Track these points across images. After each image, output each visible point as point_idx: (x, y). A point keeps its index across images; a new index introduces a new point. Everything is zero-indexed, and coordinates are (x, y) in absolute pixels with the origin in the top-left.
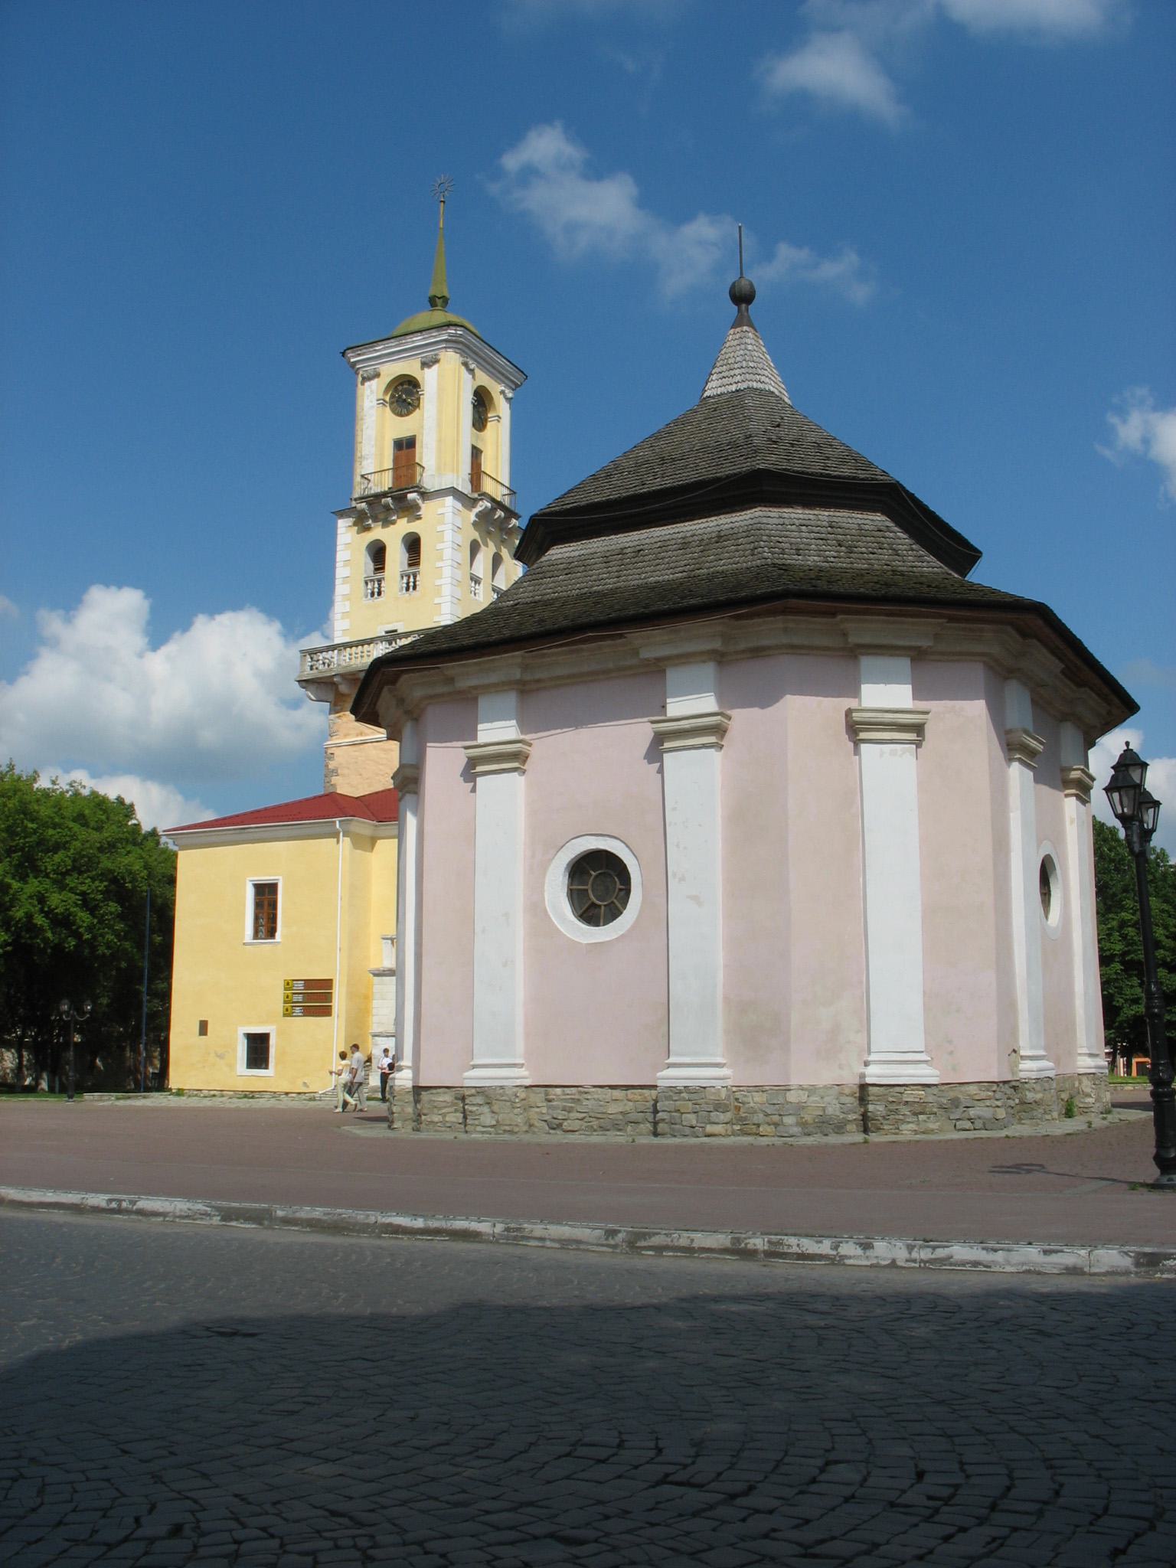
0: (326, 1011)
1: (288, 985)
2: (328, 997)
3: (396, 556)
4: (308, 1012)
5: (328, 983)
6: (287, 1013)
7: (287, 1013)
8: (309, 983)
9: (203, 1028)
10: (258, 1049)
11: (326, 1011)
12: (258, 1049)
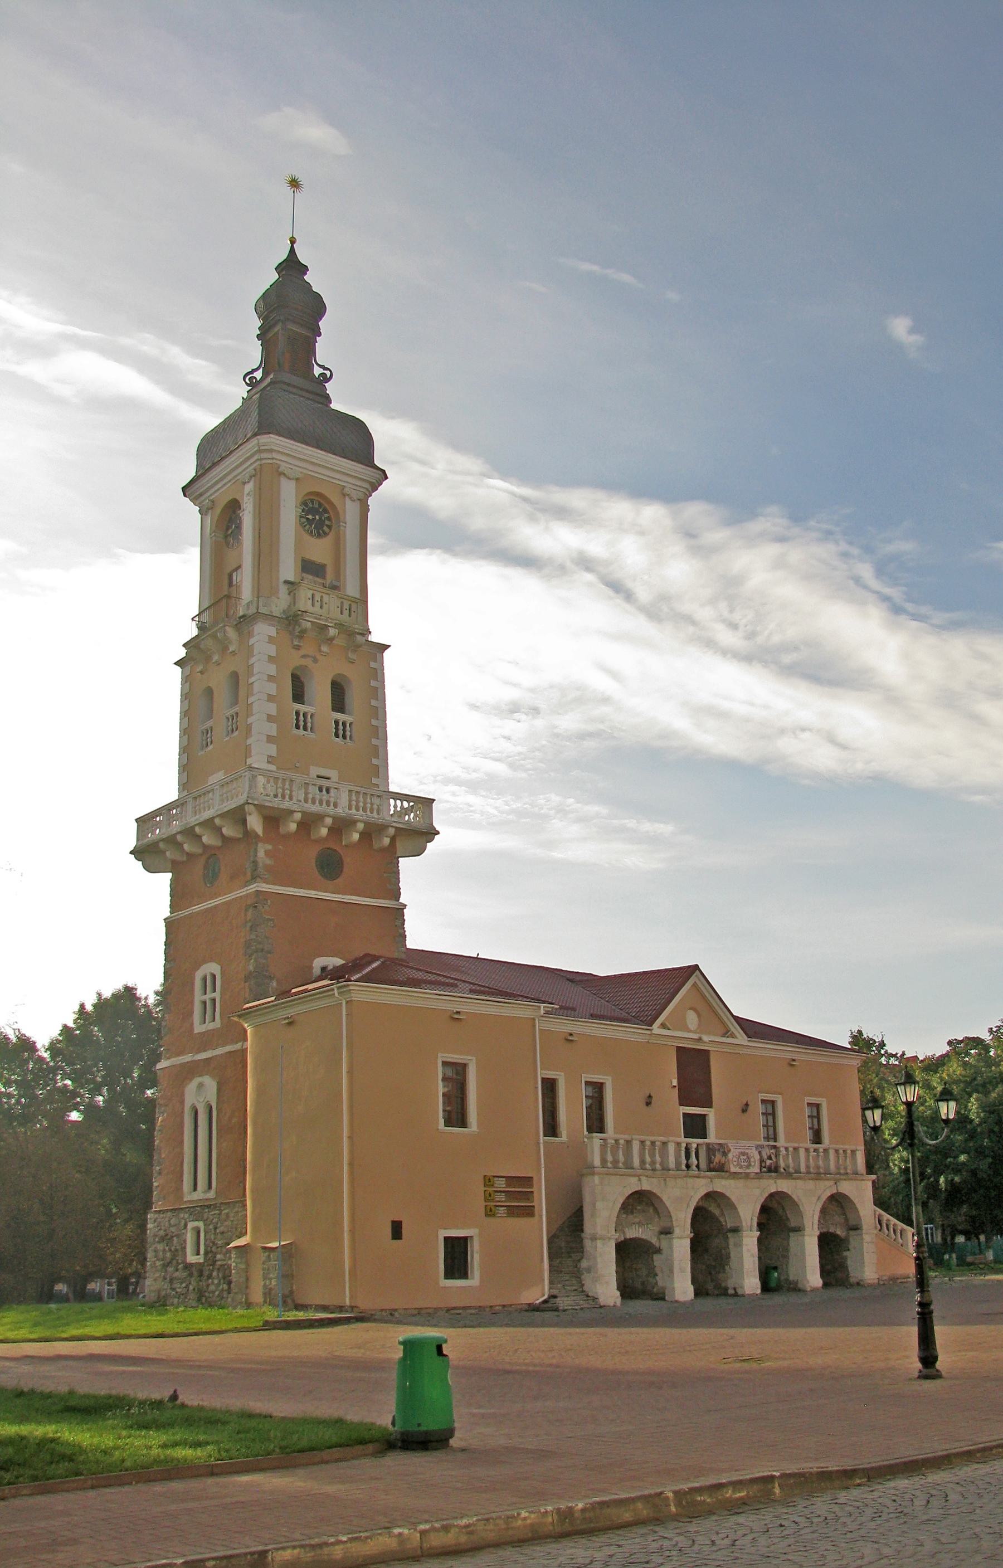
0: (529, 1212)
1: (488, 1181)
2: (528, 1195)
3: (320, 693)
4: (513, 1212)
5: (528, 1181)
6: (490, 1213)
7: (490, 1213)
8: (508, 1178)
9: (397, 1230)
10: (457, 1257)
11: (529, 1212)
12: (457, 1257)
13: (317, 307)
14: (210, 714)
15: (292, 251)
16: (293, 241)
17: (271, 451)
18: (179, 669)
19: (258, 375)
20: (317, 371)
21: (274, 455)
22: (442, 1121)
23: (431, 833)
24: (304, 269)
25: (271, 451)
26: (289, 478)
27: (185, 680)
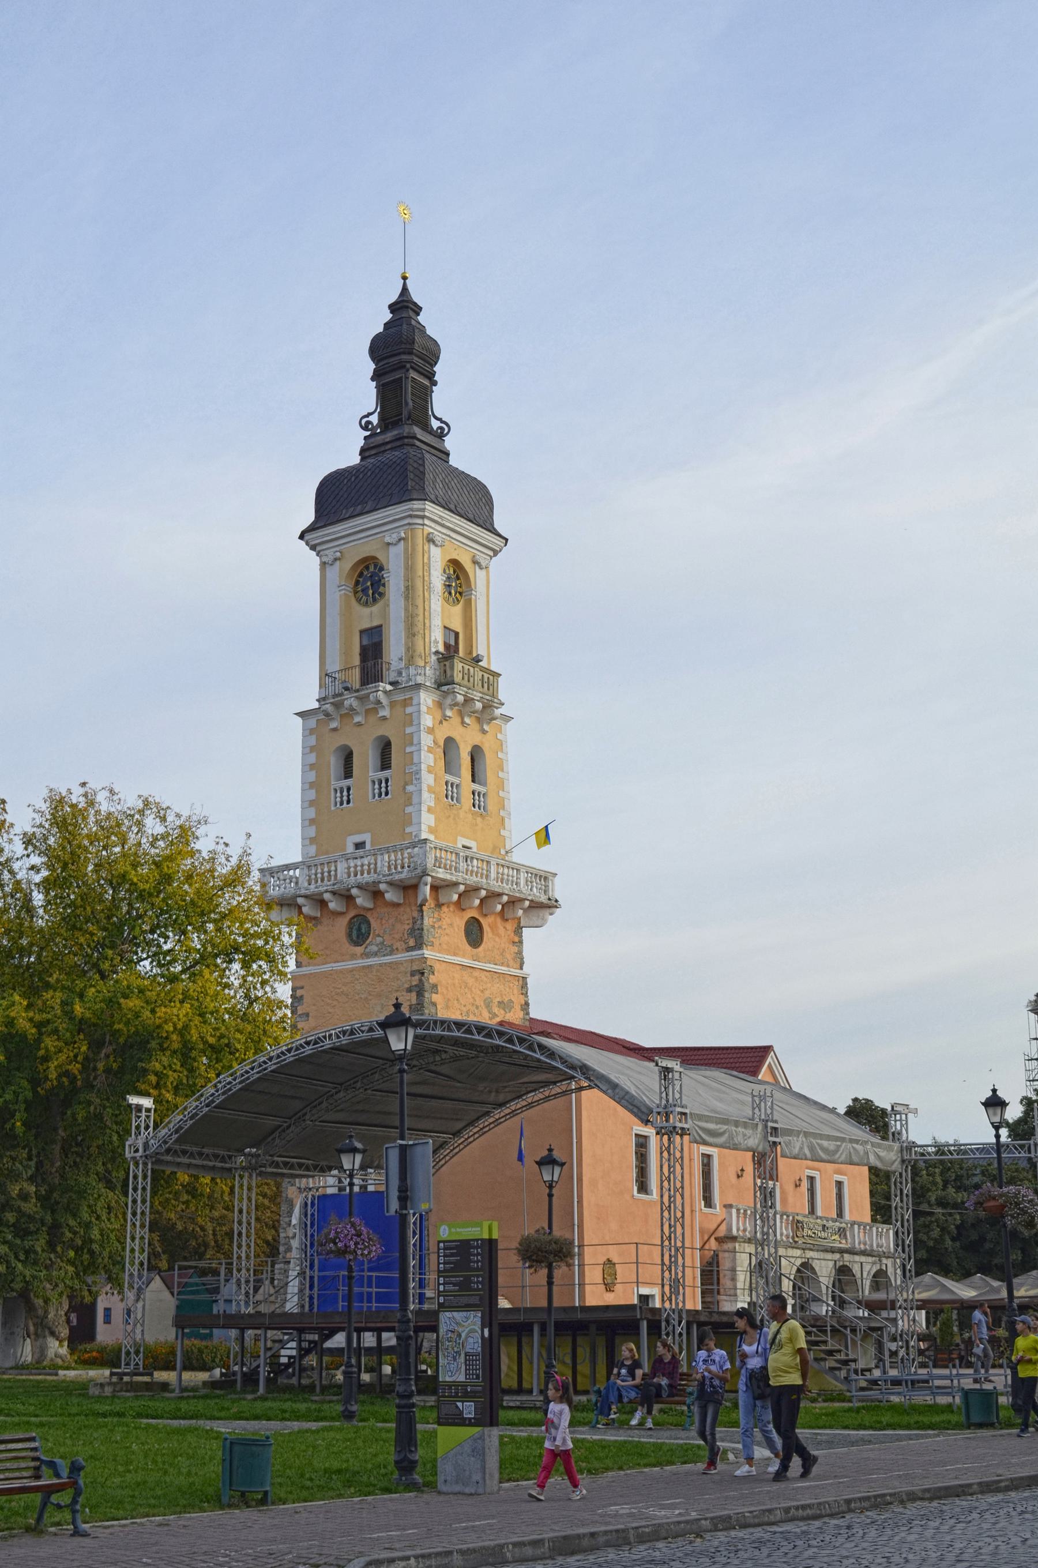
13: (431, 354)
14: (348, 774)
16: (405, 278)
17: (423, 517)
18: (299, 720)
19: (374, 419)
20: (435, 424)
21: (426, 522)
22: (635, 1188)
23: (551, 905)
24: (417, 310)
25: (423, 517)
26: (436, 546)
27: (308, 732)
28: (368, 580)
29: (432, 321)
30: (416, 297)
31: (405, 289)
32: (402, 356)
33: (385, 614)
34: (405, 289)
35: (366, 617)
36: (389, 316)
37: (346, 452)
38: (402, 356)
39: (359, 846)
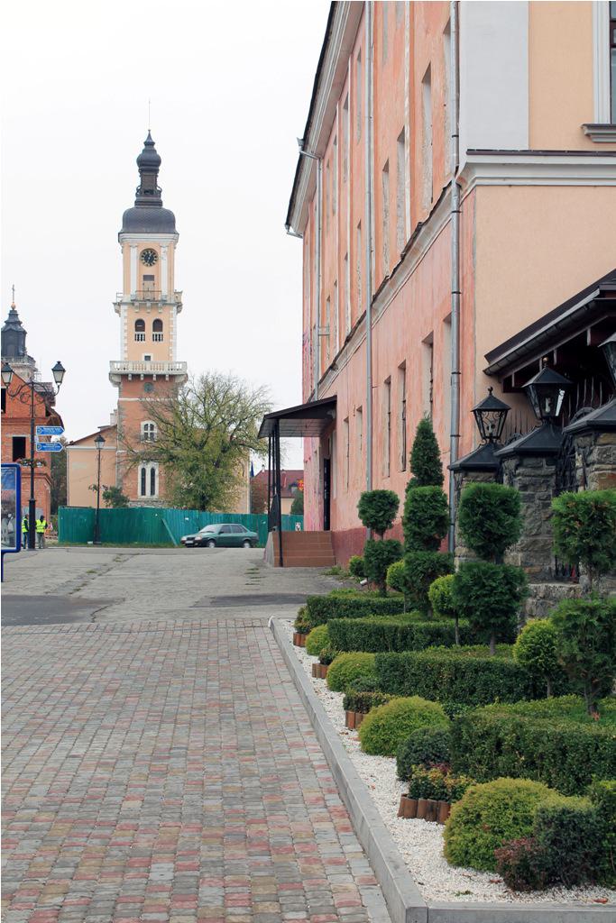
13: (158, 162)
15: (149, 135)
24: (153, 144)
28: (149, 257)
29: (159, 149)
30: (154, 140)
31: (149, 136)
32: (149, 164)
33: (158, 271)
34: (149, 136)
35: (149, 271)
36: (143, 147)
37: (129, 201)
38: (149, 164)
39: (148, 358)
